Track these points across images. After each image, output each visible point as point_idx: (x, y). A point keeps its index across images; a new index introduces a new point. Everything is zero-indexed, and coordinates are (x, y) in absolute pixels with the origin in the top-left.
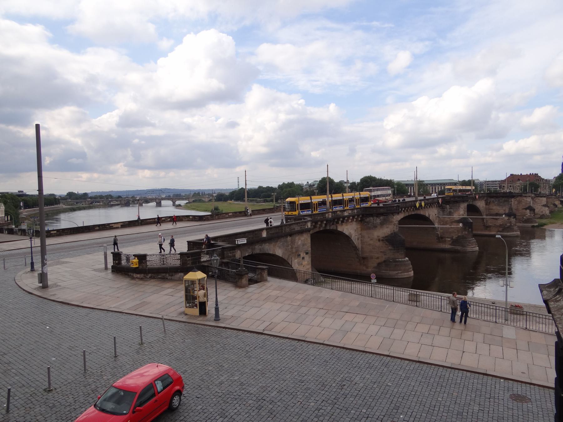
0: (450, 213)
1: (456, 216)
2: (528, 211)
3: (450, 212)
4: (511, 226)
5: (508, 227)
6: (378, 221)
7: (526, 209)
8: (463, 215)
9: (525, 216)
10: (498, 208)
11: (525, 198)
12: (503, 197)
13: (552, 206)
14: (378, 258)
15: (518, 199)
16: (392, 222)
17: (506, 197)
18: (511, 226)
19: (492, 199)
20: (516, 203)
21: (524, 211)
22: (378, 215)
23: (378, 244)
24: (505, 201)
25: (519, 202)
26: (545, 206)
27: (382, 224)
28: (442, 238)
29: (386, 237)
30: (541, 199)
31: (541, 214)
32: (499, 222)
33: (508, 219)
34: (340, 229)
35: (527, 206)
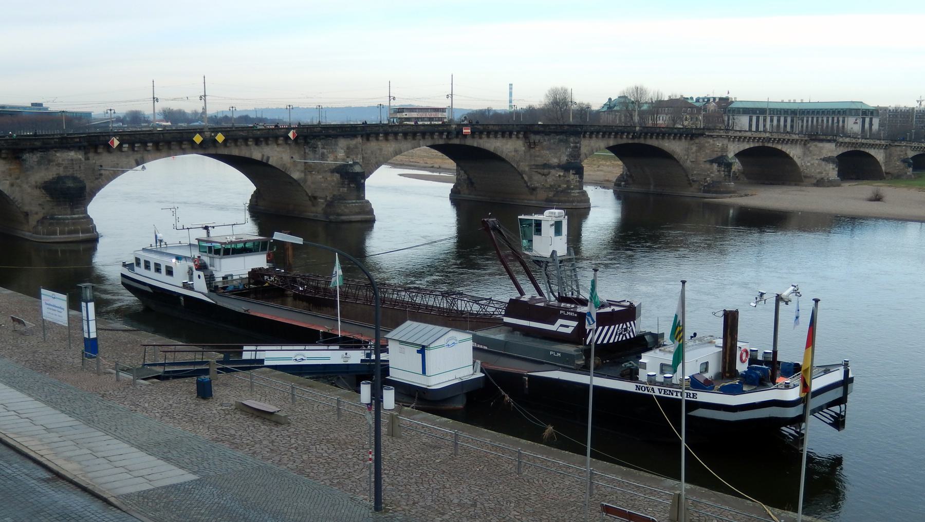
0: (323, 157)
1: (330, 162)
2: (715, 166)
3: (323, 154)
4: (568, 188)
5: (562, 191)
7: (712, 162)
8: (343, 160)
9: (708, 175)
11: (711, 141)
12: (557, 133)
14: (37, 213)
15: (697, 141)
16: (53, 161)
17: (562, 133)
20: (694, 148)
21: (708, 166)
22: (33, 150)
23: (37, 192)
27: (39, 163)
28: (315, 198)
29: (46, 182)
30: (820, 145)
31: (819, 176)
32: (550, 180)
35: (714, 156)
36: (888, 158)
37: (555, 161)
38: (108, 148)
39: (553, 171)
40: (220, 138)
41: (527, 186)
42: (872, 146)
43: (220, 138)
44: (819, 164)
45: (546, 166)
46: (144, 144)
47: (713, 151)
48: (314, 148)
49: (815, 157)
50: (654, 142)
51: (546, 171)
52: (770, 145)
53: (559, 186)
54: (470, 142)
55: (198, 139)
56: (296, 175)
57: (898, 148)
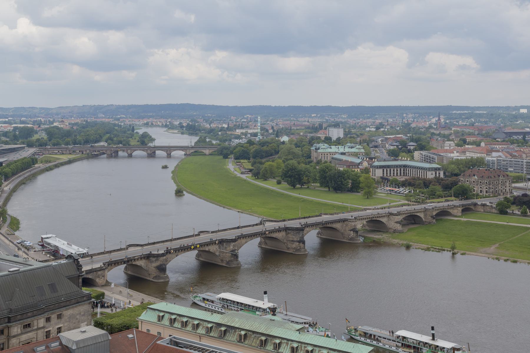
2: (352, 232)
6: (154, 259)
7: (351, 230)
13: (430, 218)
20: (344, 225)
22: (154, 257)
23: (154, 269)
26: (397, 222)
32: (294, 246)
34: (134, 263)
36: (425, 215)
37: (295, 239)
38: (170, 253)
40: (198, 246)
42: (417, 212)
43: (198, 246)
46: (179, 251)
48: (223, 245)
50: (330, 225)
54: (267, 236)
55: (192, 247)
56: (217, 254)
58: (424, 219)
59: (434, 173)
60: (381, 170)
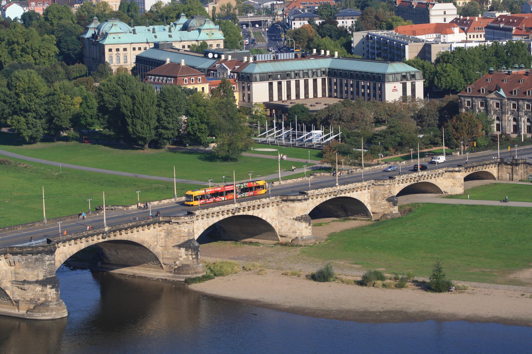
2: (183, 250)
5: (42, 304)
7: (180, 246)
9: (177, 259)
10: (26, 271)
13: (385, 202)
18: (46, 301)
19: (17, 257)
20: (163, 234)
21: (176, 250)
24: (37, 260)
25: (169, 233)
26: (299, 219)
31: (293, 236)
32: (29, 295)
33: (42, 291)
35: (182, 241)
36: (374, 197)
37: (31, 277)
39: (32, 286)
41: (10, 299)
44: (293, 225)
45: (25, 282)
47: (180, 237)
49: (289, 217)
50: (124, 236)
51: (26, 286)
52: (241, 213)
53: (39, 300)
57: (382, 188)
58: (369, 208)
59: (399, 86)
60: (266, 84)
